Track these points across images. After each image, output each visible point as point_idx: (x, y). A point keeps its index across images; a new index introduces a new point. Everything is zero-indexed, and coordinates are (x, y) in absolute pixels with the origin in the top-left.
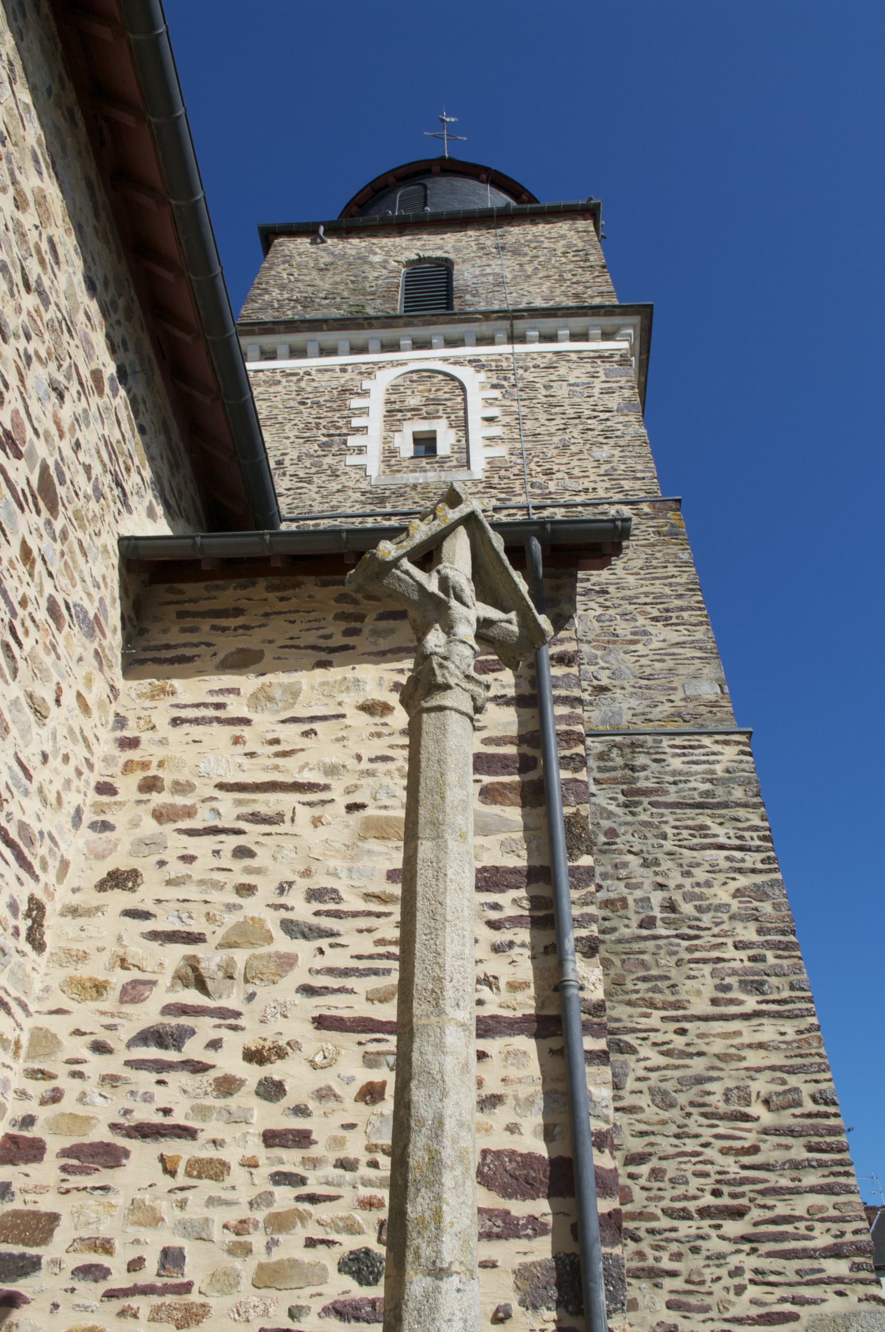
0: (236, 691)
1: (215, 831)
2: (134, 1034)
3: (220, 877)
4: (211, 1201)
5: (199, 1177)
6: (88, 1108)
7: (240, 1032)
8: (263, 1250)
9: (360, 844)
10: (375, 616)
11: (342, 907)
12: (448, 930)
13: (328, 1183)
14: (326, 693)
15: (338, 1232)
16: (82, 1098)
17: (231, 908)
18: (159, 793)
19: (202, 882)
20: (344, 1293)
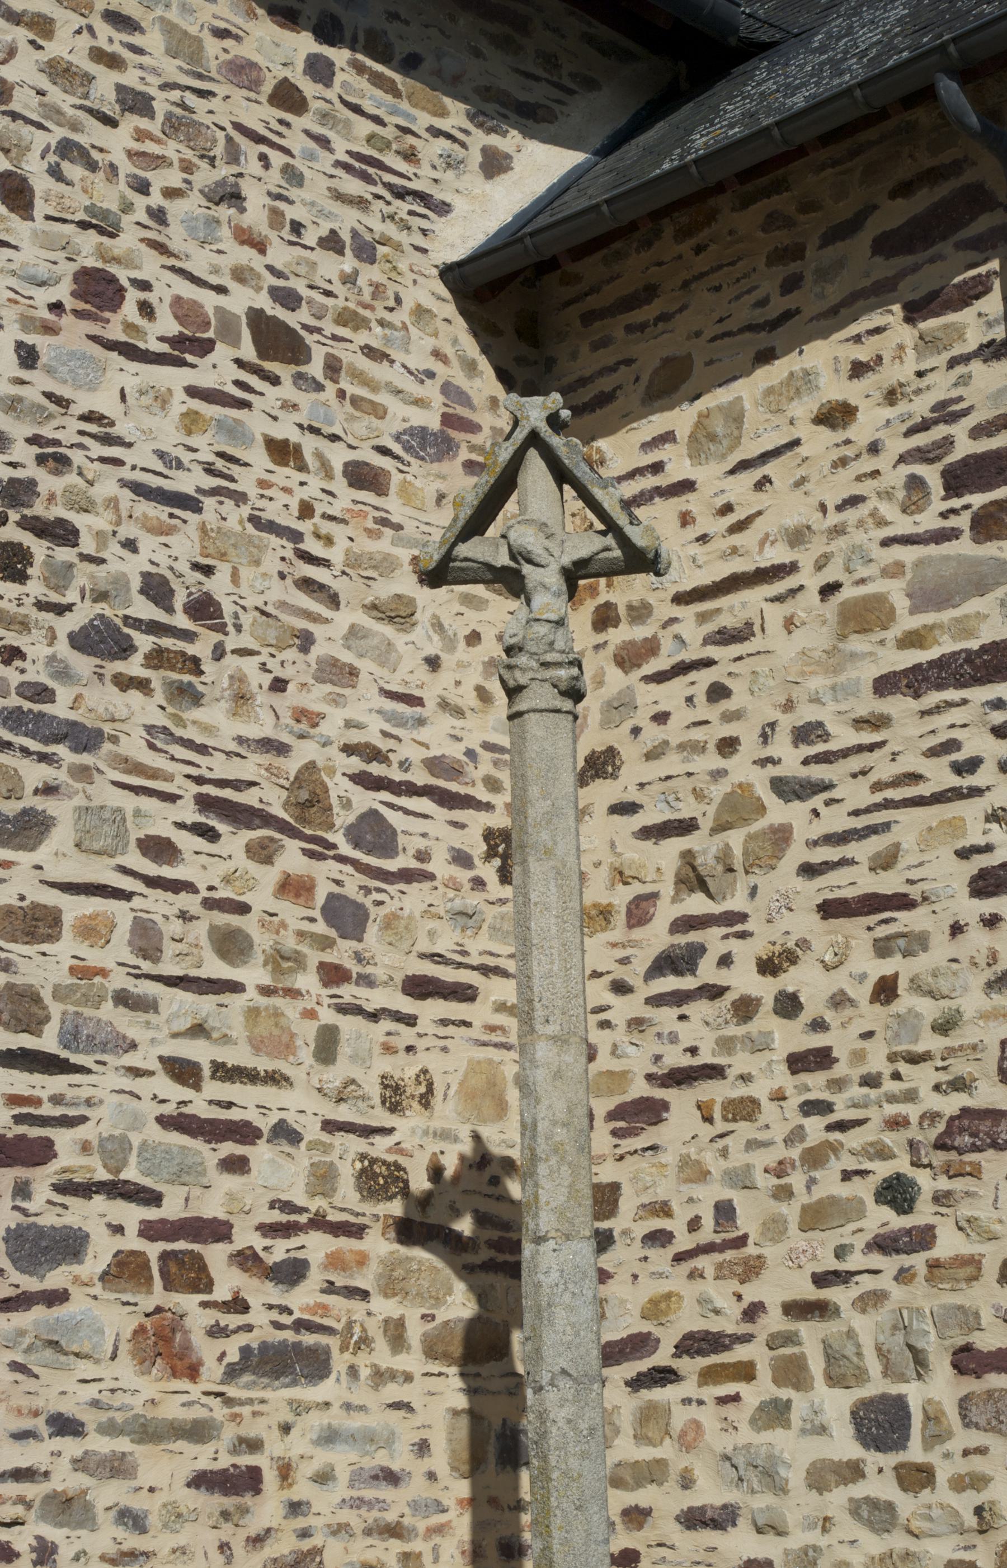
0: (668, 437)
1: (682, 669)
2: (648, 964)
3: (698, 734)
4: (752, 1145)
5: (735, 1120)
6: (623, 1061)
7: (749, 940)
8: (804, 1191)
9: (841, 645)
10: (818, 242)
11: (833, 746)
12: (535, 953)
13: (855, 1106)
14: (773, 407)
15: (871, 1160)
16: (614, 1051)
17: (717, 775)
18: (616, 627)
19: (682, 747)
20: (884, 1225)
